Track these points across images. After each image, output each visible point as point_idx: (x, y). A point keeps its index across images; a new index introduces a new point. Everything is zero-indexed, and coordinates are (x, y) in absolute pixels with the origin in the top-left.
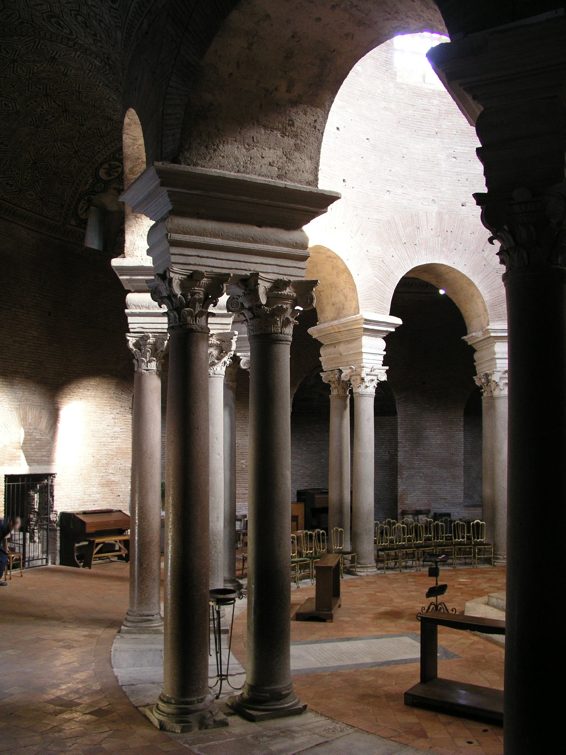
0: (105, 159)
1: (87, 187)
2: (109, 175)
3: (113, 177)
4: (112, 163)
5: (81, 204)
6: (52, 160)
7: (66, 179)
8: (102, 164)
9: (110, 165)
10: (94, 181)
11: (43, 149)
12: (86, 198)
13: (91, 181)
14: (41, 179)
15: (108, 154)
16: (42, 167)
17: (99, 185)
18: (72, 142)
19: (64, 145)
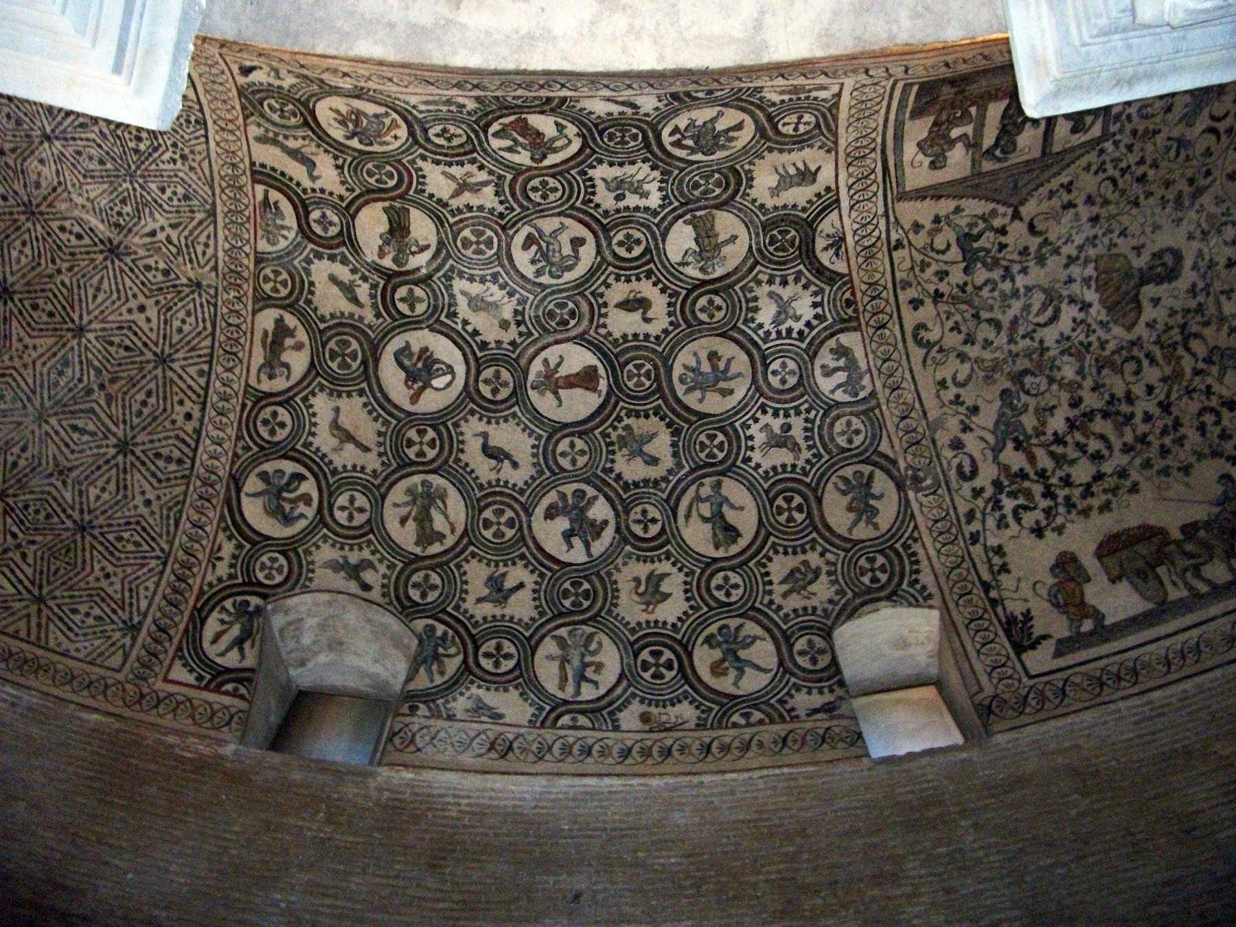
0: (235, 455)
1: (223, 569)
2: (287, 520)
3: (302, 524)
4: (269, 467)
5: (212, 626)
6: (59, 484)
7: (130, 547)
8: (236, 481)
9: (264, 476)
10: (239, 546)
11: (16, 450)
12: (228, 604)
13: (228, 549)
14: (33, 542)
15: (232, 432)
16: (26, 507)
17: (264, 559)
18: (93, 411)
19: (75, 428)
